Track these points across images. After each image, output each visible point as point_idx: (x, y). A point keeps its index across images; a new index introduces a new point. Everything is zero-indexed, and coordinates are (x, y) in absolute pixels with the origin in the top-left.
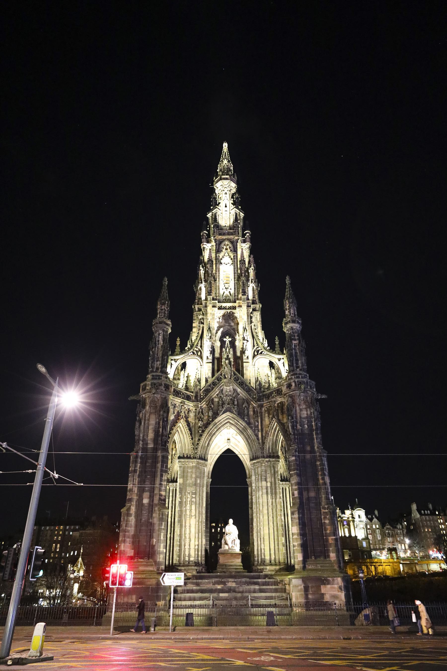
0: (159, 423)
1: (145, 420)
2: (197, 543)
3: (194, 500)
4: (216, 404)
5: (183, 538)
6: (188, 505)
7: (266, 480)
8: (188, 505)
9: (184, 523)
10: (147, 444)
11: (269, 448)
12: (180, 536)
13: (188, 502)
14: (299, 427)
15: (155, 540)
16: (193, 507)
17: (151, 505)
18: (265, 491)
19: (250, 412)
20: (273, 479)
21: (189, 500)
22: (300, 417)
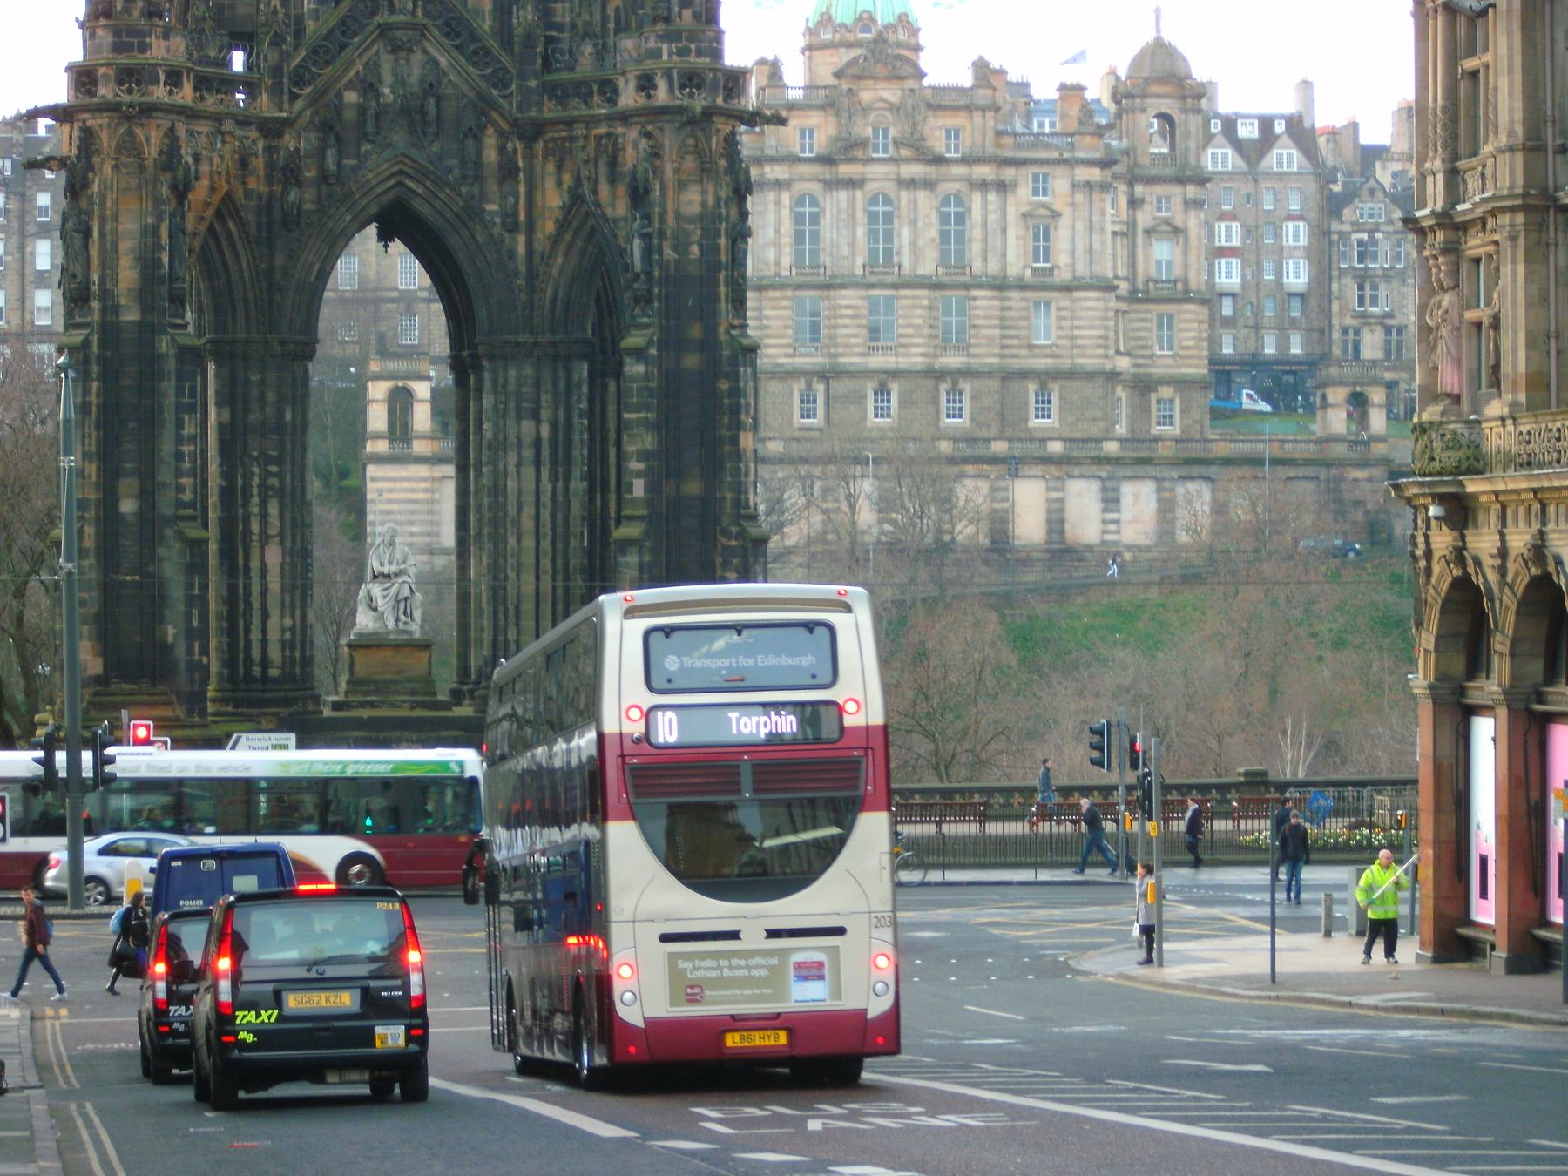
0: (155, 231)
1: (103, 220)
2: (288, 622)
3: (274, 482)
4: (350, 115)
5: (242, 606)
6: (256, 500)
7: (536, 416)
8: (256, 500)
9: (241, 561)
10: (116, 309)
11: (554, 301)
12: (231, 599)
13: (255, 491)
14: (669, 253)
15: (171, 631)
16: (273, 510)
17: (149, 520)
18: (528, 453)
19: (485, 153)
20: (561, 413)
21: (256, 481)
22: (678, 216)
